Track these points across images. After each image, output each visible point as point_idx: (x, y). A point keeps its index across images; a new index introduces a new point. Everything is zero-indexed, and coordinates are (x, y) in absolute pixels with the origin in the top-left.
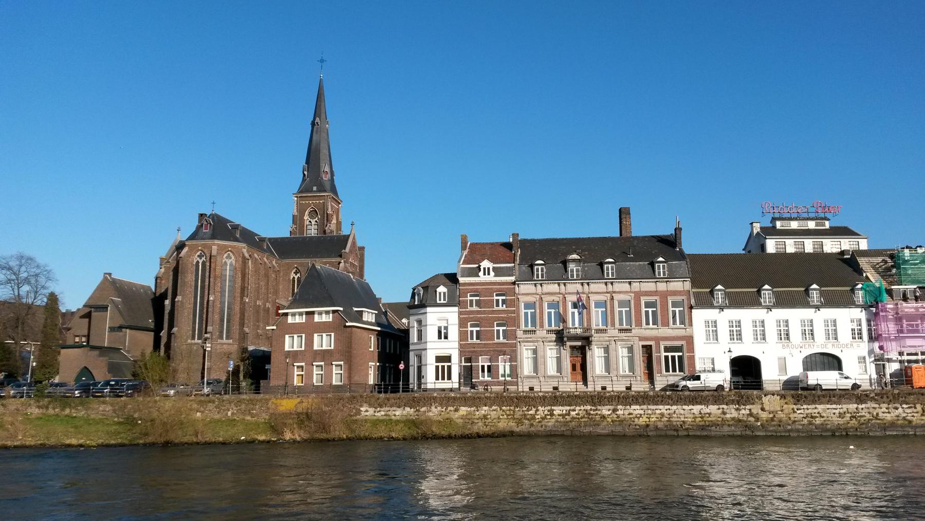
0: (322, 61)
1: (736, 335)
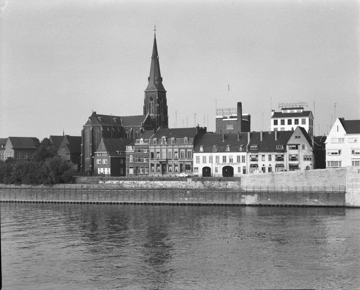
0: (155, 30)
1: (204, 161)
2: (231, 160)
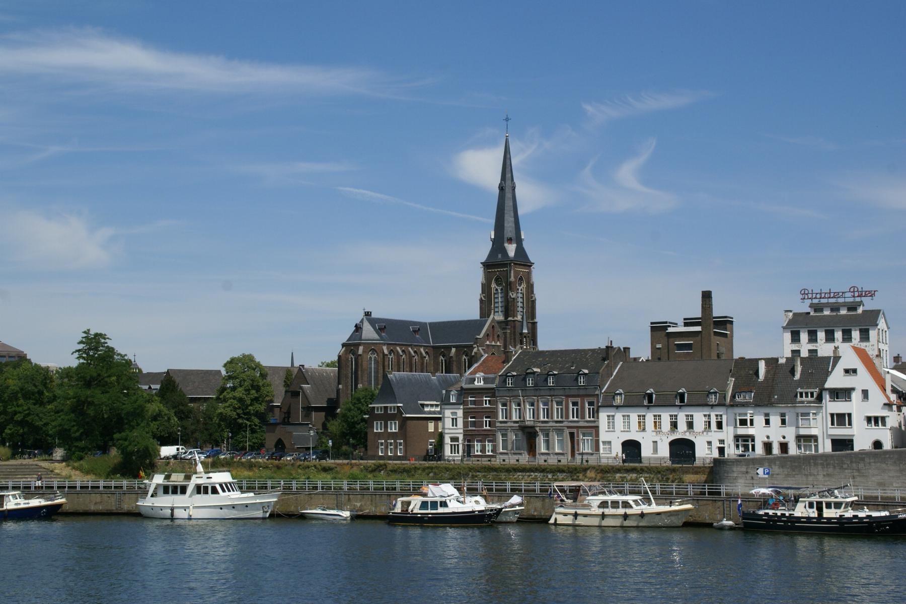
0: (507, 119)
2: (690, 425)
